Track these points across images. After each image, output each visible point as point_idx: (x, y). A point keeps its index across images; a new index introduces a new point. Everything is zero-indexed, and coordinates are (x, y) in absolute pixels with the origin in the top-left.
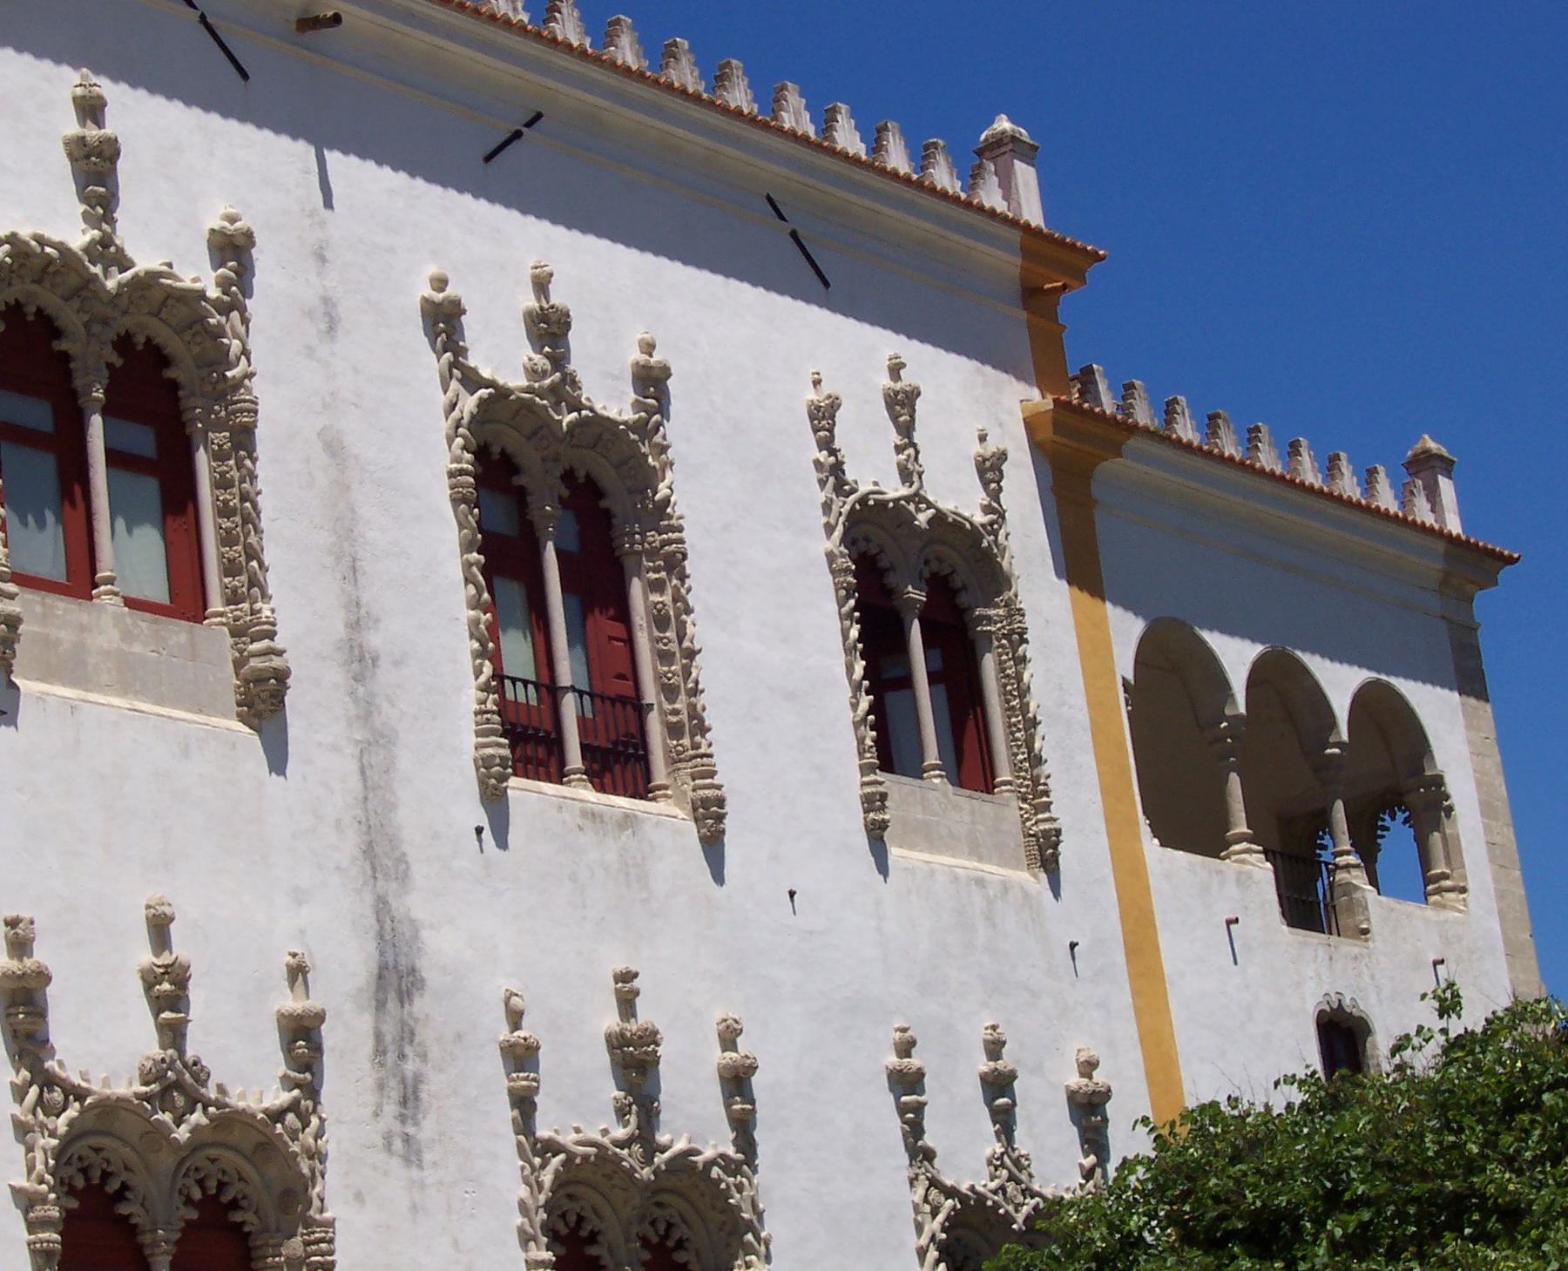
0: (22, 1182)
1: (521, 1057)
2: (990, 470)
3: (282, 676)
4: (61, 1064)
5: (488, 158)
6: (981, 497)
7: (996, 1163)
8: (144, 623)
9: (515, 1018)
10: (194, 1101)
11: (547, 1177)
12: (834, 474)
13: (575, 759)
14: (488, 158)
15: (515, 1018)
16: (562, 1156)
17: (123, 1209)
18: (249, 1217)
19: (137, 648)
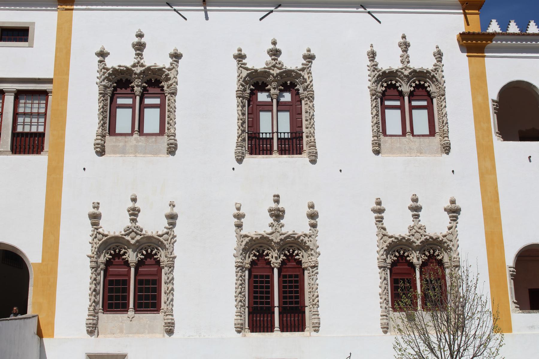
0: (90, 254)
1: (239, 217)
2: (439, 55)
3: (176, 145)
4: (103, 230)
5: (261, 19)
6: (435, 61)
7: (411, 228)
8: (143, 138)
9: (238, 209)
10: (137, 234)
11: (244, 243)
12: (375, 67)
13: (275, 147)
14: (261, 19)
15: (238, 209)
16: (249, 238)
17: (124, 257)
18: (159, 256)
19: (140, 144)
